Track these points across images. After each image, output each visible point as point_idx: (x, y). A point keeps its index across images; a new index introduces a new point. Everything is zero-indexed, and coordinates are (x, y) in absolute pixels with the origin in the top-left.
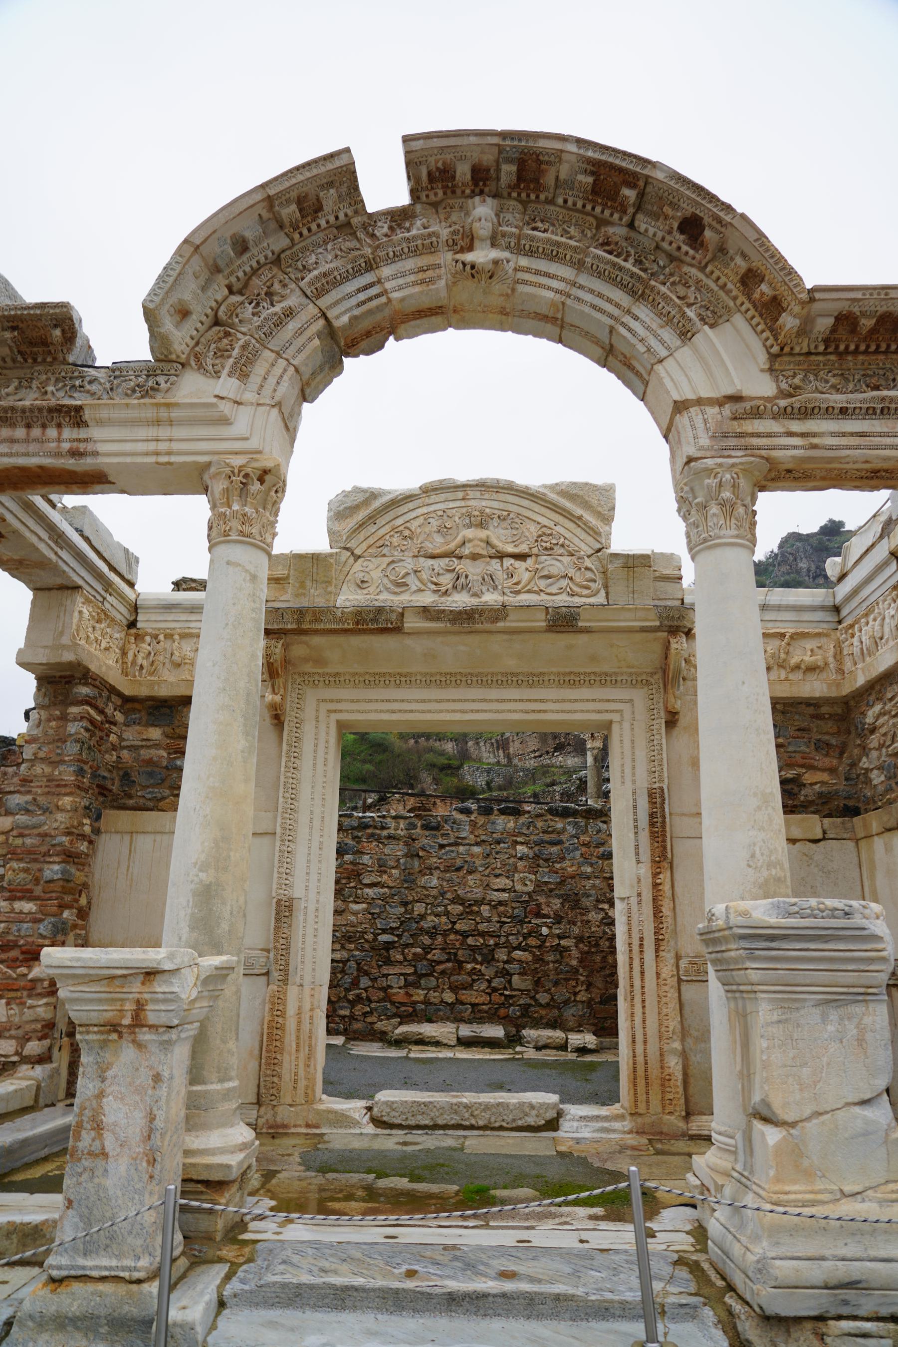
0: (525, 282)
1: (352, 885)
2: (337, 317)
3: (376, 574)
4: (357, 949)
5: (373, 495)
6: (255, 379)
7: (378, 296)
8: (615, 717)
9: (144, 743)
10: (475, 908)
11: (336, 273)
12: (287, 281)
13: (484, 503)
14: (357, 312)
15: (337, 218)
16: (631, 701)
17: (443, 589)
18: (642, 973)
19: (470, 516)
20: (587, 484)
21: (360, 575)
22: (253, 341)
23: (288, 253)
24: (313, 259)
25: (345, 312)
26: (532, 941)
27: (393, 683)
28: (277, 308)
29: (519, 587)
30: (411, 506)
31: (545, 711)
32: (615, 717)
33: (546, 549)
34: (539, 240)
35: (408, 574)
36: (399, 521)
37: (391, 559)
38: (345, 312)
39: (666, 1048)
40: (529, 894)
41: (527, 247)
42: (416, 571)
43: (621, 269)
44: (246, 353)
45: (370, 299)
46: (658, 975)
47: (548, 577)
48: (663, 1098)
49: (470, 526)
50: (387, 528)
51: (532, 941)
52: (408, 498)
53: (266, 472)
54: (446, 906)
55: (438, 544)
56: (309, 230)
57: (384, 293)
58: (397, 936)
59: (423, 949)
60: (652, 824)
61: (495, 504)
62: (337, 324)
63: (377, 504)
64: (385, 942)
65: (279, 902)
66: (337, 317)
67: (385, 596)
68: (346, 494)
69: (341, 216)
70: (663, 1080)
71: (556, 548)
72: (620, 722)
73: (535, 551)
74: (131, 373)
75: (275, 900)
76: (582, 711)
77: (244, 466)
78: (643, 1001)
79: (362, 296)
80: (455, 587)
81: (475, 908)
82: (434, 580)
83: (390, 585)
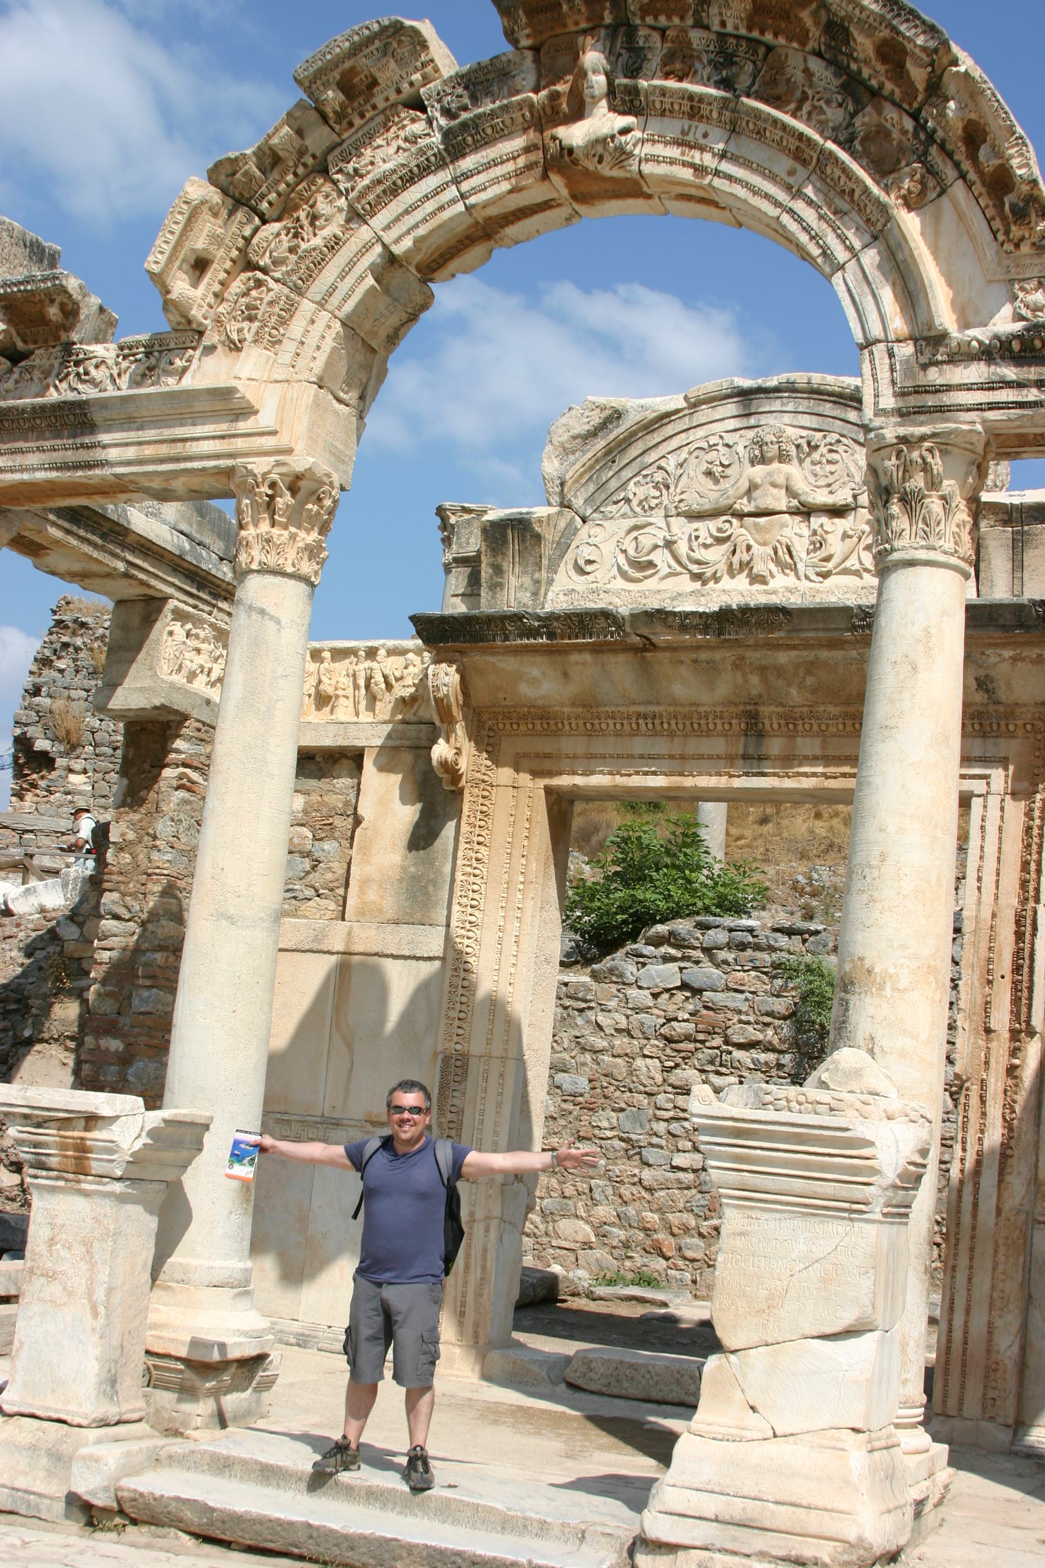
0: (655, 159)
1: (714, 1043)
2: (397, 241)
3: (609, 548)
6: (289, 347)
7: (453, 202)
11: (395, 177)
12: (334, 194)
13: (787, 418)
14: (421, 231)
15: (399, 91)
17: (709, 572)
19: (761, 444)
22: (286, 291)
23: (336, 152)
24: (366, 159)
25: (408, 232)
29: (830, 565)
30: (669, 430)
34: (673, 92)
35: (656, 547)
37: (631, 522)
38: (408, 232)
39: (999, 1322)
41: (658, 105)
43: (784, 127)
44: (277, 310)
45: (441, 208)
46: (999, 1211)
53: (298, 477)
55: (709, 495)
57: (463, 196)
60: (1017, 969)
62: (398, 250)
63: (618, 431)
65: (446, 1060)
66: (397, 241)
67: (620, 583)
69: (405, 87)
74: (142, 349)
75: (440, 1057)
77: (269, 472)
78: (972, 1249)
79: (430, 206)
82: (696, 555)
83: (626, 568)
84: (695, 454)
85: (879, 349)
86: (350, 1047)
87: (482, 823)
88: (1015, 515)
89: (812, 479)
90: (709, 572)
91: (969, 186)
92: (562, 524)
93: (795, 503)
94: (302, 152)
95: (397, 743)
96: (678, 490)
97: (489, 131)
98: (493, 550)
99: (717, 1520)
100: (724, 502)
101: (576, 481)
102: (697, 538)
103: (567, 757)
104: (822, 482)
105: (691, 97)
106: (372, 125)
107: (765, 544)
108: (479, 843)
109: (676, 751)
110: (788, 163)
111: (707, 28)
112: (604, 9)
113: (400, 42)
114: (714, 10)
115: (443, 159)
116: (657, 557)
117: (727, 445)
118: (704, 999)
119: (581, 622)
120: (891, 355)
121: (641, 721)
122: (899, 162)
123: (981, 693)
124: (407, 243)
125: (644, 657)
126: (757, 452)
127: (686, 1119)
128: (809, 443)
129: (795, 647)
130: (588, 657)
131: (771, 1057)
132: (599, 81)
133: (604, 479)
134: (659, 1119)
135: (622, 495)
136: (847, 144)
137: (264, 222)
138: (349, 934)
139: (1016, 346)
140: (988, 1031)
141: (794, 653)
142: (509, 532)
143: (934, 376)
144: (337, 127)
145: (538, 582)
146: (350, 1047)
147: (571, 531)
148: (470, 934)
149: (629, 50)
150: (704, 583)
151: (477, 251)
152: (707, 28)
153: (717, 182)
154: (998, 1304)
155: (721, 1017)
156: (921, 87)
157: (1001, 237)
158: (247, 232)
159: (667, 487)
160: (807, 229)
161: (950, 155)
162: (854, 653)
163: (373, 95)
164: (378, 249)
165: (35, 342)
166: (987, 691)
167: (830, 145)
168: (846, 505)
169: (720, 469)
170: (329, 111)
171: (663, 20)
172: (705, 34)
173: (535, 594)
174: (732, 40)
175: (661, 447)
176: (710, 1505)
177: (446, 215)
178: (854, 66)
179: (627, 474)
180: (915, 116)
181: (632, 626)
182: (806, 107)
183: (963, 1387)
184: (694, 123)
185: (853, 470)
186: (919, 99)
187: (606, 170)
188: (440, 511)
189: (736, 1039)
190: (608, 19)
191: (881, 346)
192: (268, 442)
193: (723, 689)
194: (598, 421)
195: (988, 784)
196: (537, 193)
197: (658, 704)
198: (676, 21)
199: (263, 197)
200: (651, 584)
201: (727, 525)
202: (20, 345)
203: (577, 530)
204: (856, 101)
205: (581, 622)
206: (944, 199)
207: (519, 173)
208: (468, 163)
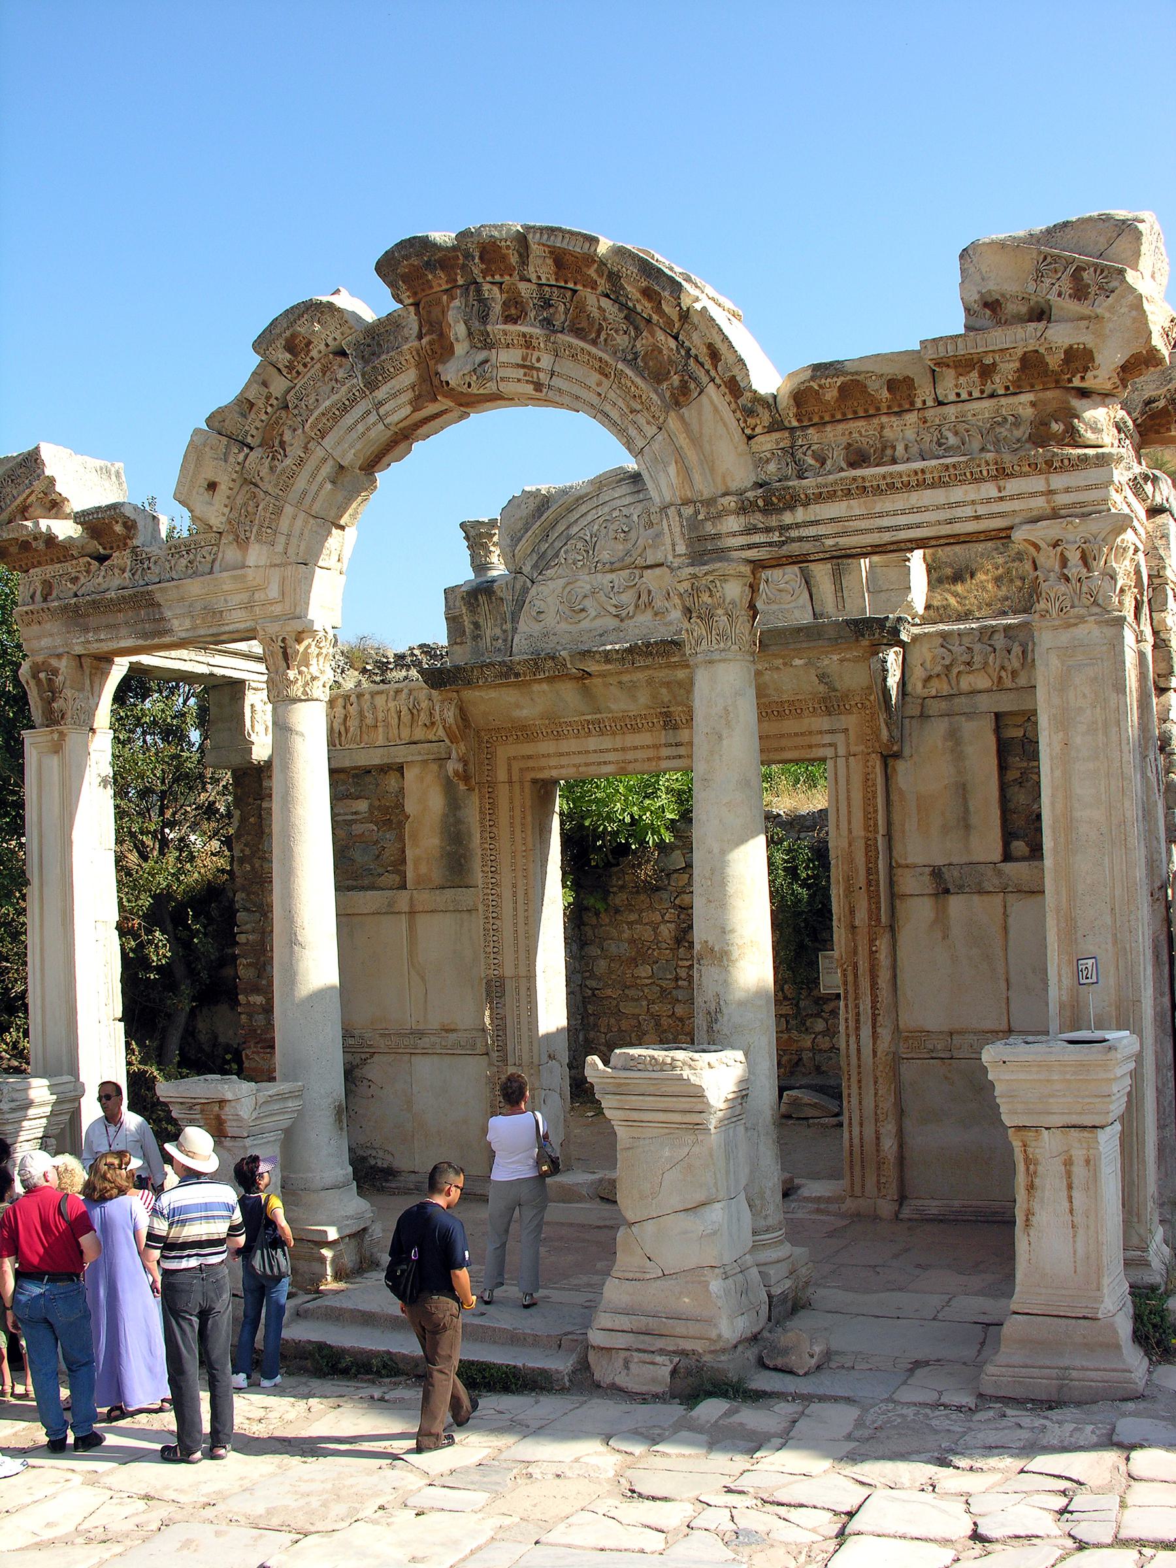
5: (542, 503)
8: (829, 752)
9: (354, 817)
14: (359, 446)
15: (327, 345)
16: (847, 730)
17: (624, 613)
18: (859, 1051)
23: (292, 393)
28: (288, 461)
30: (583, 509)
32: (829, 752)
37: (563, 581)
39: (882, 1130)
48: (878, 1182)
52: (580, 499)
56: (305, 365)
67: (564, 626)
70: (878, 1163)
76: (790, 749)
78: (859, 1081)
79: (361, 428)
80: (637, 606)
82: (614, 602)
85: (672, 511)
86: (423, 978)
90: (624, 613)
91: (719, 387)
92: (518, 587)
94: (268, 398)
95: (426, 757)
97: (392, 370)
99: (632, 1332)
105: (524, 335)
106: (312, 371)
109: (619, 746)
110: (596, 376)
111: (529, 281)
112: (456, 274)
113: (322, 313)
114: (531, 269)
115: (364, 392)
116: (588, 603)
120: (680, 515)
122: (669, 372)
124: (350, 455)
130: (545, 686)
132: (460, 330)
136: (632, 362)
137: (252, 449)
138: (411, 898)
139: (761, 503)
140: (854, 927)
143: (709, 528)
144: (289, 376)
145: (505, 631)
146: (423, 978)
147: (525, 591)
149: (479, 301)
150: (622, 621)
151: (403, 446)
152: (529, 281)
153: (551, 393)
154: (881, 1117)
156: (675, 318)
157: (743, 425)
158: (241, 457)
160: (615, 424)
161: (702, 365)
163: (309, 351)
164: (330, 462)
165: (112, 548)
166: (826, 683)
167: (620, 366)
170: (280, 366)
171: (497, 278)
172: (528, 285)
173: (505, 640)
174: (547, 289)
176: (624, 1322)
177: (373, 434)
178: (630, 304)
180: (676, 338)
182: (603, 336)
183: (863, 1176)
184: (530, 352)
186: (676, 326)
187: (474, 390)
188: (462, 525)
190: (460, 282)
191: (673, 508)
192: (277, 609)
193: (643, 698)
196: (432, 409)
198: (507, 278)
199: (247, 432)
200: (585, 624)
202: (102, 551)
204: (636, 328)
206: (703, 396)
207: (417, 398)
208: (380, 394)
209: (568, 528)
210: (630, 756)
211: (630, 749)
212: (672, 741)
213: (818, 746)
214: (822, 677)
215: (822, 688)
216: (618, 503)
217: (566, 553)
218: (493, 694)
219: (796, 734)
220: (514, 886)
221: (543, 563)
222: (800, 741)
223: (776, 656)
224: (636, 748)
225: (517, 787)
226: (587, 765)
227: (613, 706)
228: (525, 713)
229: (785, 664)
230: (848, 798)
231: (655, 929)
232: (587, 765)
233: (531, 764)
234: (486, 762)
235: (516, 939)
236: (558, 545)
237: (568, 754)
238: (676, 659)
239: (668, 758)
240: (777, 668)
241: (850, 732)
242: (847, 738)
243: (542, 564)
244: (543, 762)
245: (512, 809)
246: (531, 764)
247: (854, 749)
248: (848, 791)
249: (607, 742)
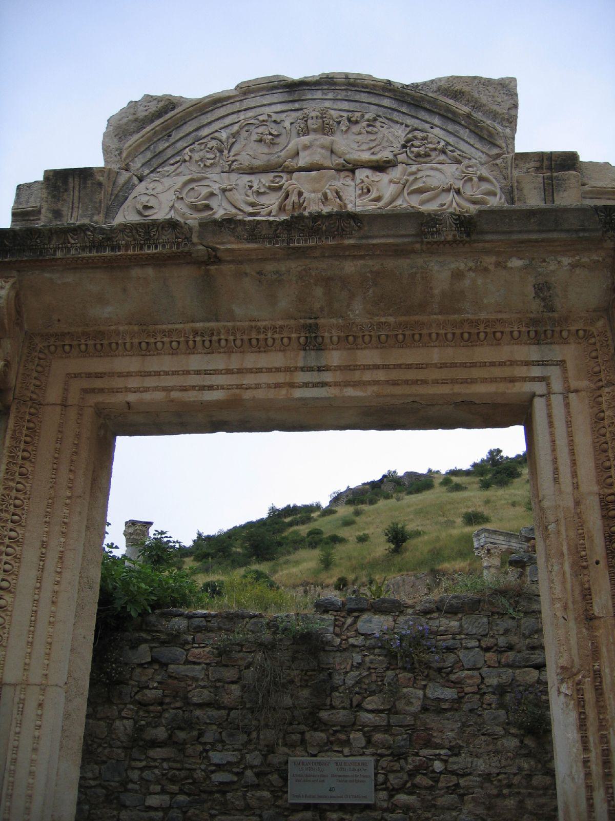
1: (178, 704)
4: (182, 792)
5: (168, 104)
10: (343, 737)
13: (327, 104)
16: (562, 363)
19: (305, 119)
20: (475, 78)
21: (144, 199)
26: (418, 779)
27: (182, 346)
31: (424, 382)
32: (539, 388)
33: (418, 155)
36: (205, 132)
40: (415, 716)
42: (224, 191)
47: (420, 191)
49: (306, 131)
50: (190, 140)
51: (418, 779)
52: (217, 101)
54: (303, 733)
55: (259, 155)
58: (237, 774)
59: (272, 792)
61: (345, 105)
64: (221, 783)
68: (133, 105)
71: (433, 154)
72: (547, 395)
73: (402, 157)
76: (484, 380)
81: (343, 737)
82: (251, 199)
84: (246, 128)
87: (28, 439)
88: (546, 163)
89: (355, 146)
92: (122, 180)
93: (342, 161)
96: (232, 154)
98: (54, 197)
100: (274, 159)
101: (136, 149)
102: (251, 187)
103: (120, 375)
104: (365, 147)
107: (314, 192)
108: (23, 458)
117: (275, 121)
118: (170, 670)
119: (147, 233)
121: (198, 339)
123: (538, 301)
125: (208, 271)
126: (302, 126)
127: (156, 767)
128: (349, 120)
129: (362, 257)
130: (150, 271)
131: (223, 712)
133: (161, 148)
134: (134, 768)
135: (178, 158)
140: (589, 619)
141: (362, 262)
142: (71, 180)
147: (129, 187)
148: (10, 550)
155: (183, 684)
159: (221, 151)
162: (420, 261)
166: (543, 299)
168: (389, 162)
169: (270, 137)
175: (213, 125)
179: (180, 145)
181: (201, 236)
185: (391, 139)
189: (195, 700)
193: (285, 301)
194: (154, 109)
195: (548, 385)
197: (217, 320)
201: (277, 180)
203: (134, 186)
205: (147, 233)
209: (197, 129)
210: (249, 379)
211: (250, 371)
212: (313, 364)
213: (524, 379)
214: (543, 289)
215: (536, 306)
216: (268, 110)
217: (192, 151)
218: (70, 278)
219: (493, 364)
220: (44, 545)
221: (157, 162)
222: (497, 372)
223: (488, 252)
224: (259, 371)
225: (72, 414)
226: (184, 389)
227: (238, 311)
228: (107, 311)
229: (498, 264)
230: (571, 443)
231: (110, 726)
232: (184, 389)
233: (98, 383)
234: (35, 374)
235: (33, 623)
236: (180, 145)
237: (158, 374)
238: (352, 241)
239: (306, 385)
240: (486, 270)
241: (570, 365)
242: (565, 371)
243: (155, 163)
244: (119, 383)
245: (59, 441)
246: (98, 383)
247: (574, 384)
248: (570, 435)
249: (218, 362)
